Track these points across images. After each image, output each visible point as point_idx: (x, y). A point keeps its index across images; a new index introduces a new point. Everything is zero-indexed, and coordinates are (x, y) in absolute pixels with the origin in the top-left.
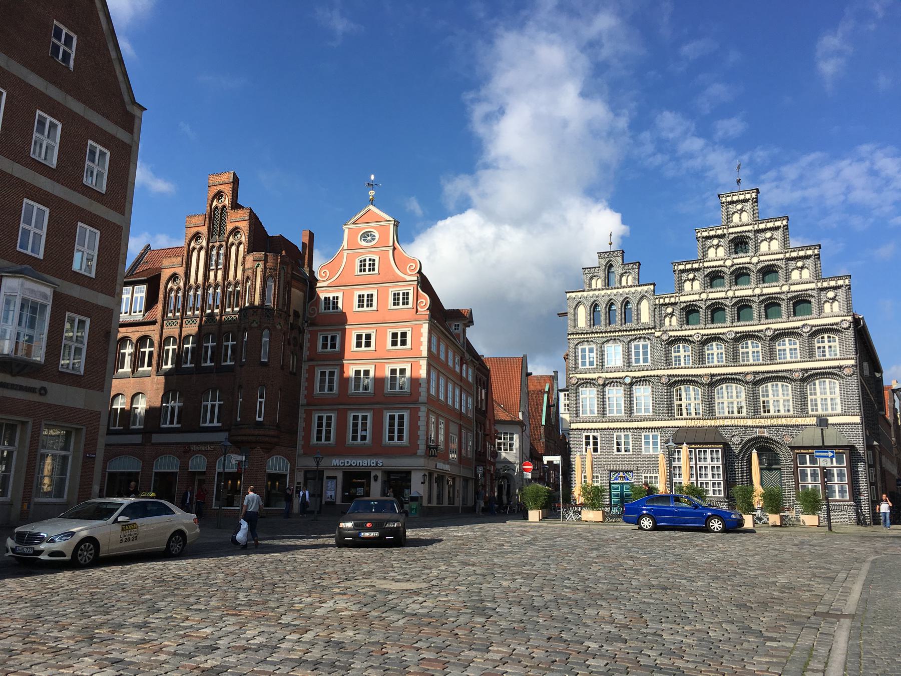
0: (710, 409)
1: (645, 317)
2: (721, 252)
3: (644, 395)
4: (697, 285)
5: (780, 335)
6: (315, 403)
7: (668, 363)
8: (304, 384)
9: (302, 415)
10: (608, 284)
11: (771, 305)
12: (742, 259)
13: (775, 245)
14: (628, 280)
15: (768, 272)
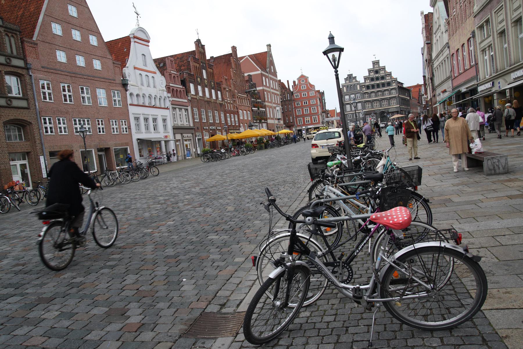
0: (372, 107)
1: (358, 88)
2: (373, 73)
3: (359, 105)
4: (368, 81)
5: (385, 90)
6: (297, 117)
7: (364, 98)
8: (294, 113)
9: (295, 119)
10: (350, 82)
11: (383, 85)
12: (377, 75)
13: (383, 72)
14: (354, 81)
15: (383, 78)
